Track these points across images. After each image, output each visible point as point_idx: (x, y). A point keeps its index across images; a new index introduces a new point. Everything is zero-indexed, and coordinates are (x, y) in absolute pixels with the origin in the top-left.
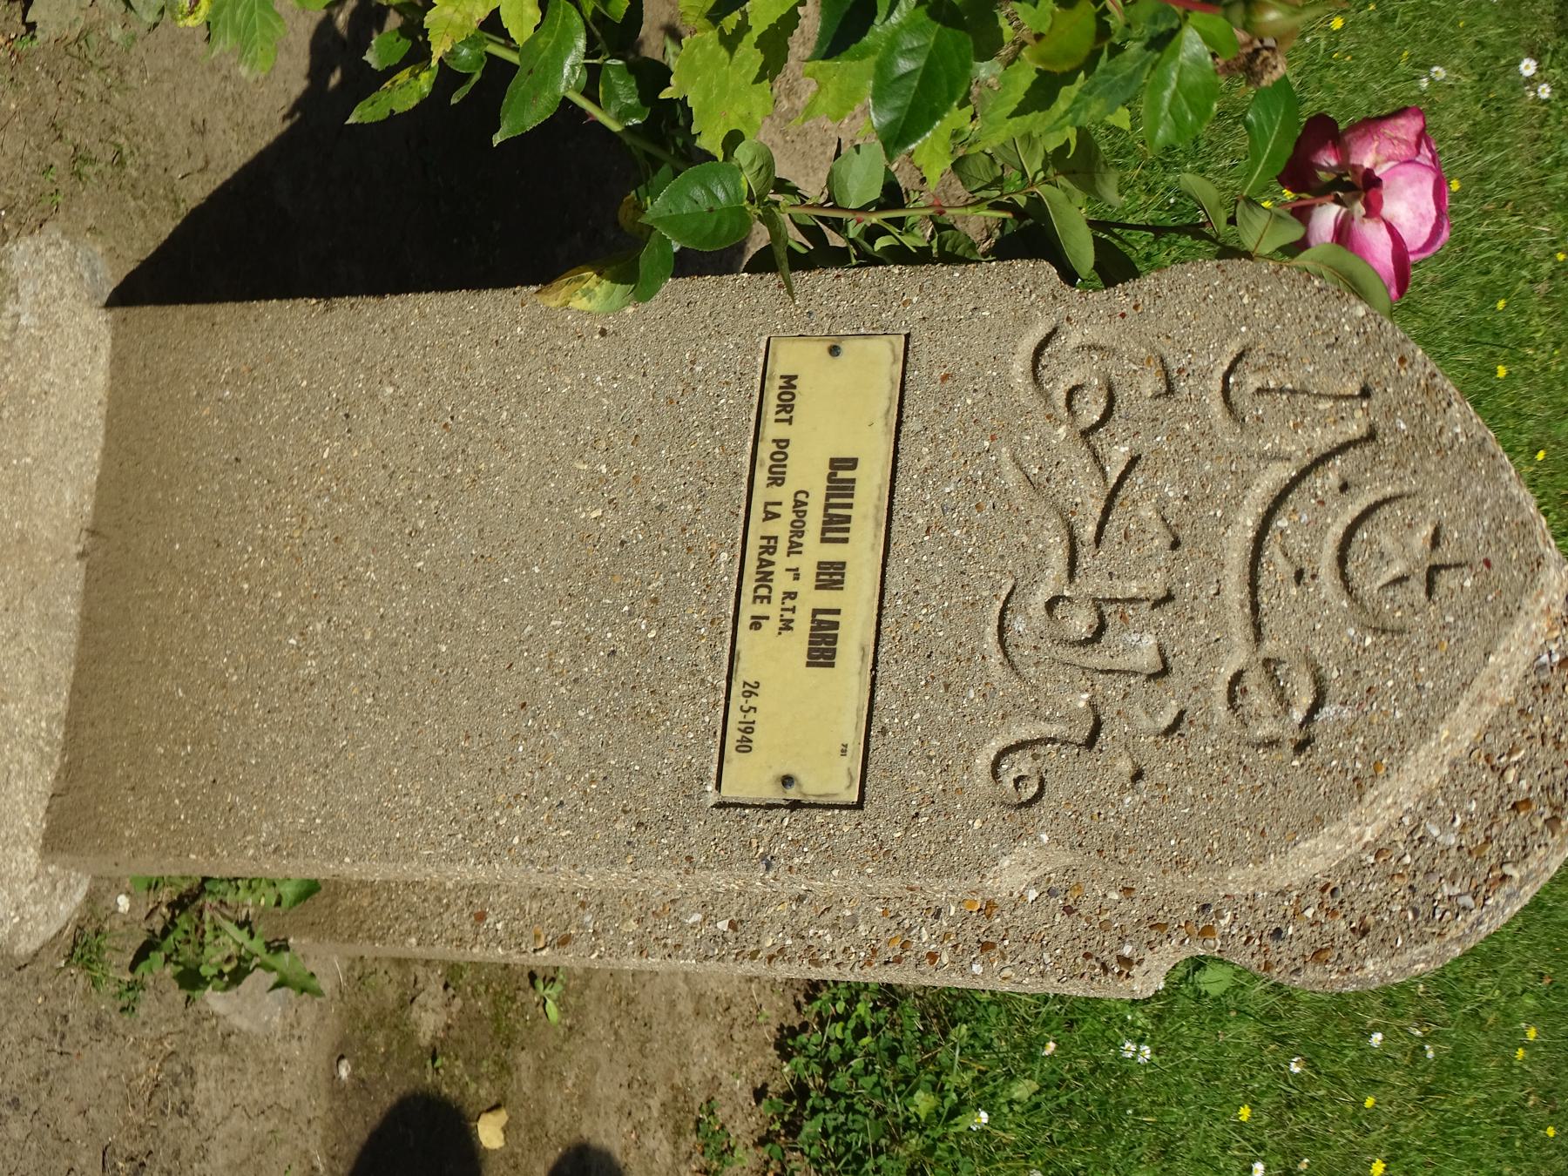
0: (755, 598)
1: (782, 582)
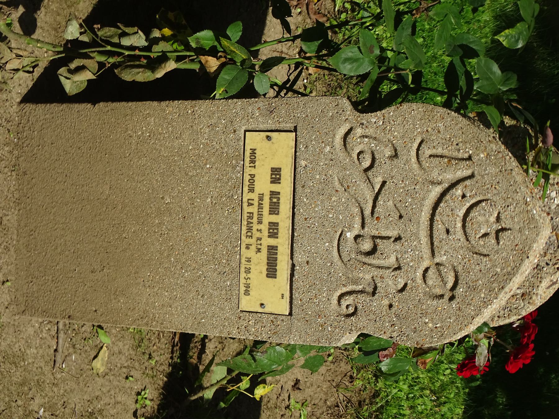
0: (247, 236)
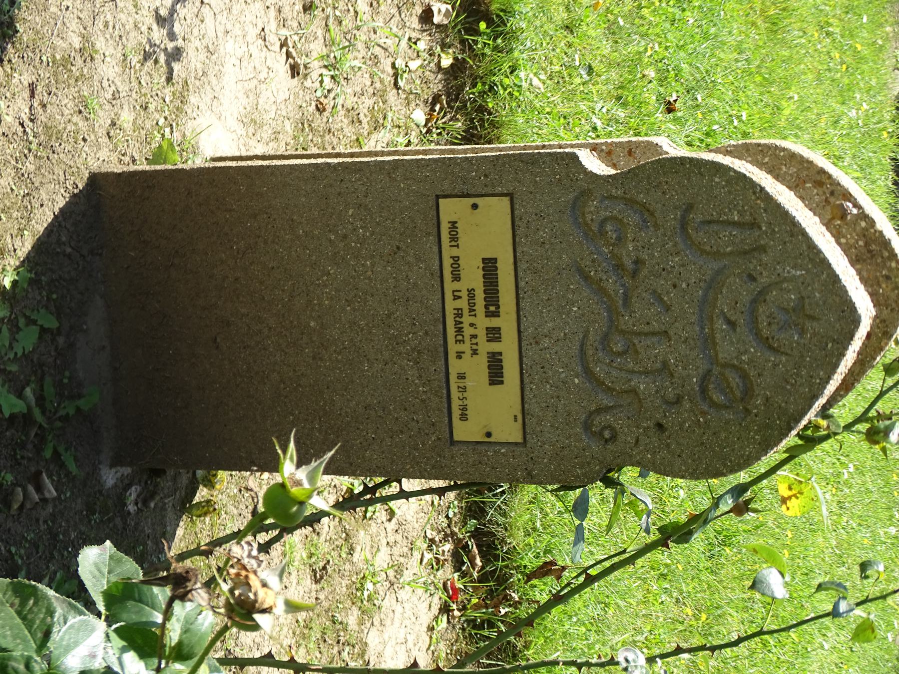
0: (456, 341)
1: (468, 331)
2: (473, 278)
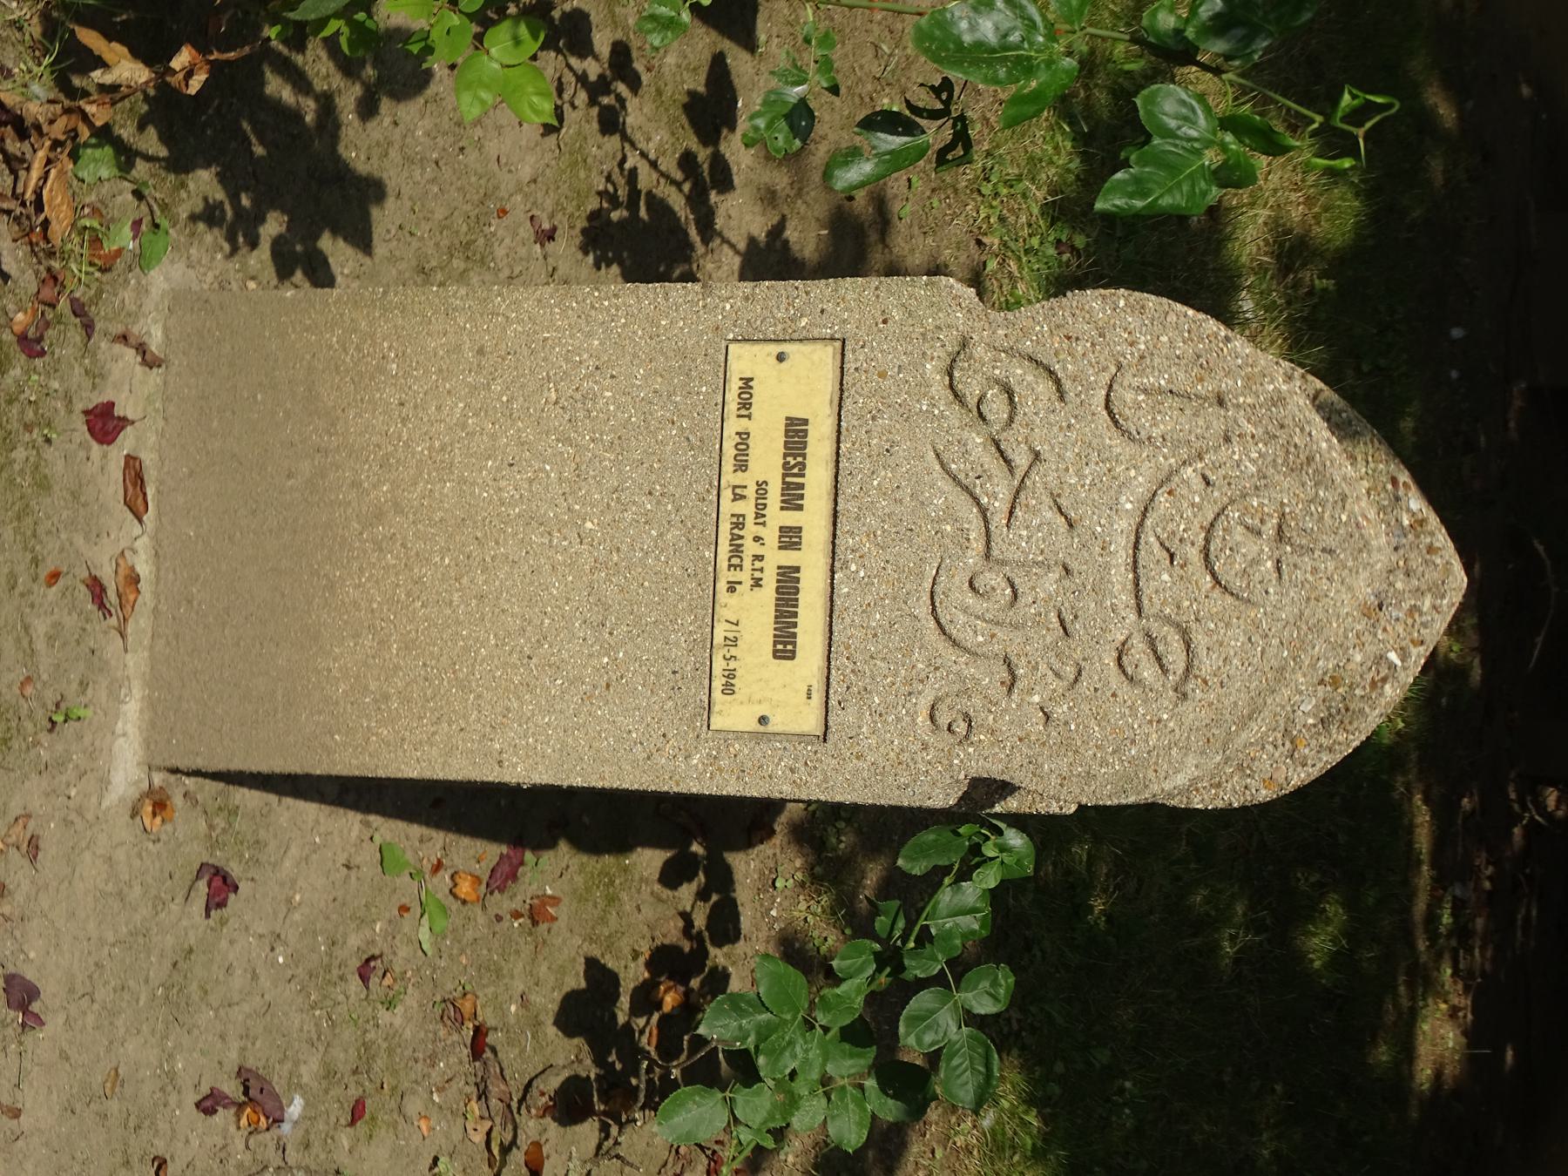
0: (730, 566)
1: (750, 548)
2: (767, 462)
